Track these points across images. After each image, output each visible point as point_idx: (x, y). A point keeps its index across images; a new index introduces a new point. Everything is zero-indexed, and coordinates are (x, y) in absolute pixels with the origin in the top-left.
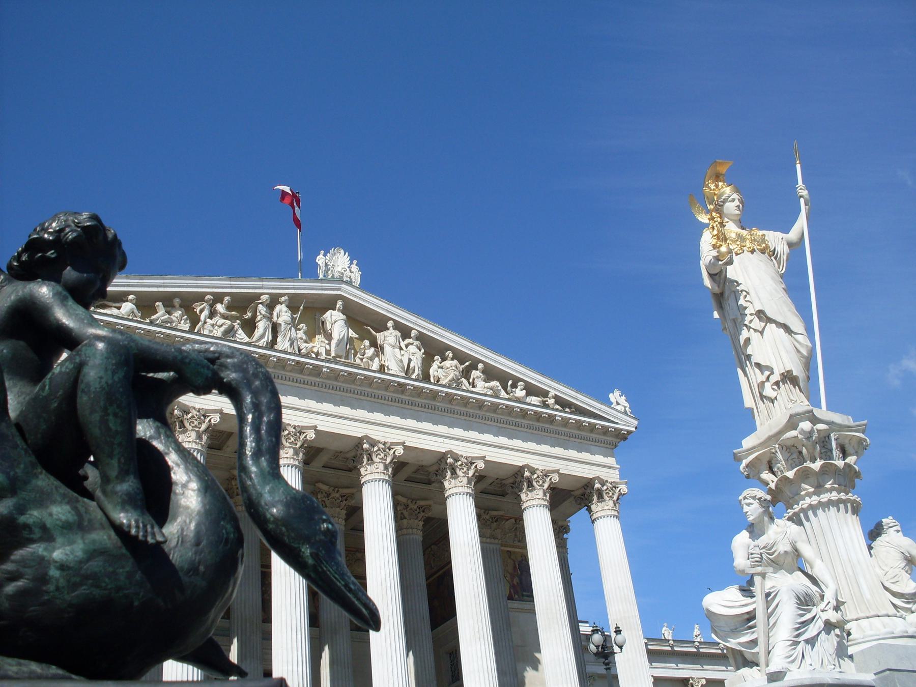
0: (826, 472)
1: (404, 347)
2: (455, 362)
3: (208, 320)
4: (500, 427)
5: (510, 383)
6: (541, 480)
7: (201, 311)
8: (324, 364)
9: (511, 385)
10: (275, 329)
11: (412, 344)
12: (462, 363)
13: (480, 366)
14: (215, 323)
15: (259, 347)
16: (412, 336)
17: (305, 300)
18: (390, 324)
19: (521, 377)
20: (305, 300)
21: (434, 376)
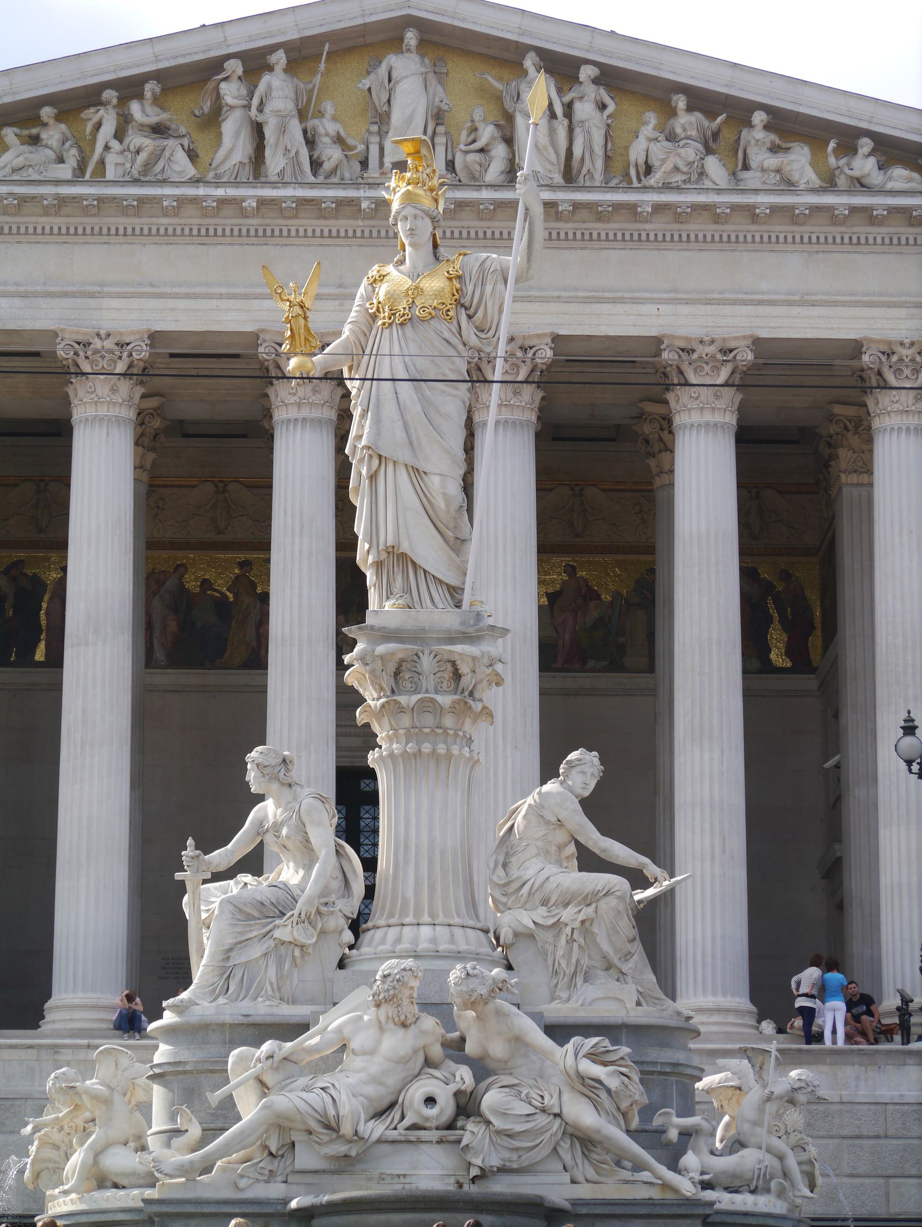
0: (403, 710)
1: (559, 110)
2: (697, 117)
3: (115, 145)
4: (809, 252)
5: (832, 145)
6: (907, 367)
7: (98, 125)
8: (361, 193)
9: (834, 150)
10: (258, 130)
11: (581, 98)
12: (711, 115)
13: (759, 118)
14: (126, 147)
15: (217, 185)
16: (581, 80)
17: (327, 47)
18: (529, 62)
19: (864, 125)
20: (327, 47)
21: (637, 165)
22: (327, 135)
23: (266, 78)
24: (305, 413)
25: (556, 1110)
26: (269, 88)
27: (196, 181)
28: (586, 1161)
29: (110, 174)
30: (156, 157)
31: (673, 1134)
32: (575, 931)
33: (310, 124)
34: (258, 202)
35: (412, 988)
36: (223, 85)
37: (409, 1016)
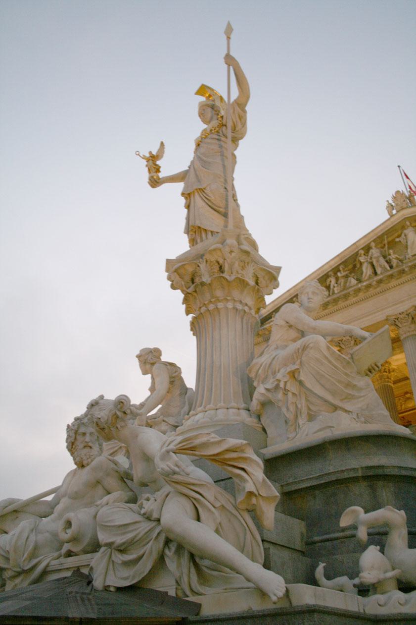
3: (336, 285)
22: (393, 258)
23: (371, 251)
24: (408, 334)
25: (155, 515)
26: (372, 253)
27: (357, 284)
28: (193, 570)
29: (336, 292)
30: (345, 283)
31: (362, 534)
32: (287, 383)
33: (388, 258)
34: (376, 282)
35: (84, 434)
36: (360, 258)
37: (85, 458)
